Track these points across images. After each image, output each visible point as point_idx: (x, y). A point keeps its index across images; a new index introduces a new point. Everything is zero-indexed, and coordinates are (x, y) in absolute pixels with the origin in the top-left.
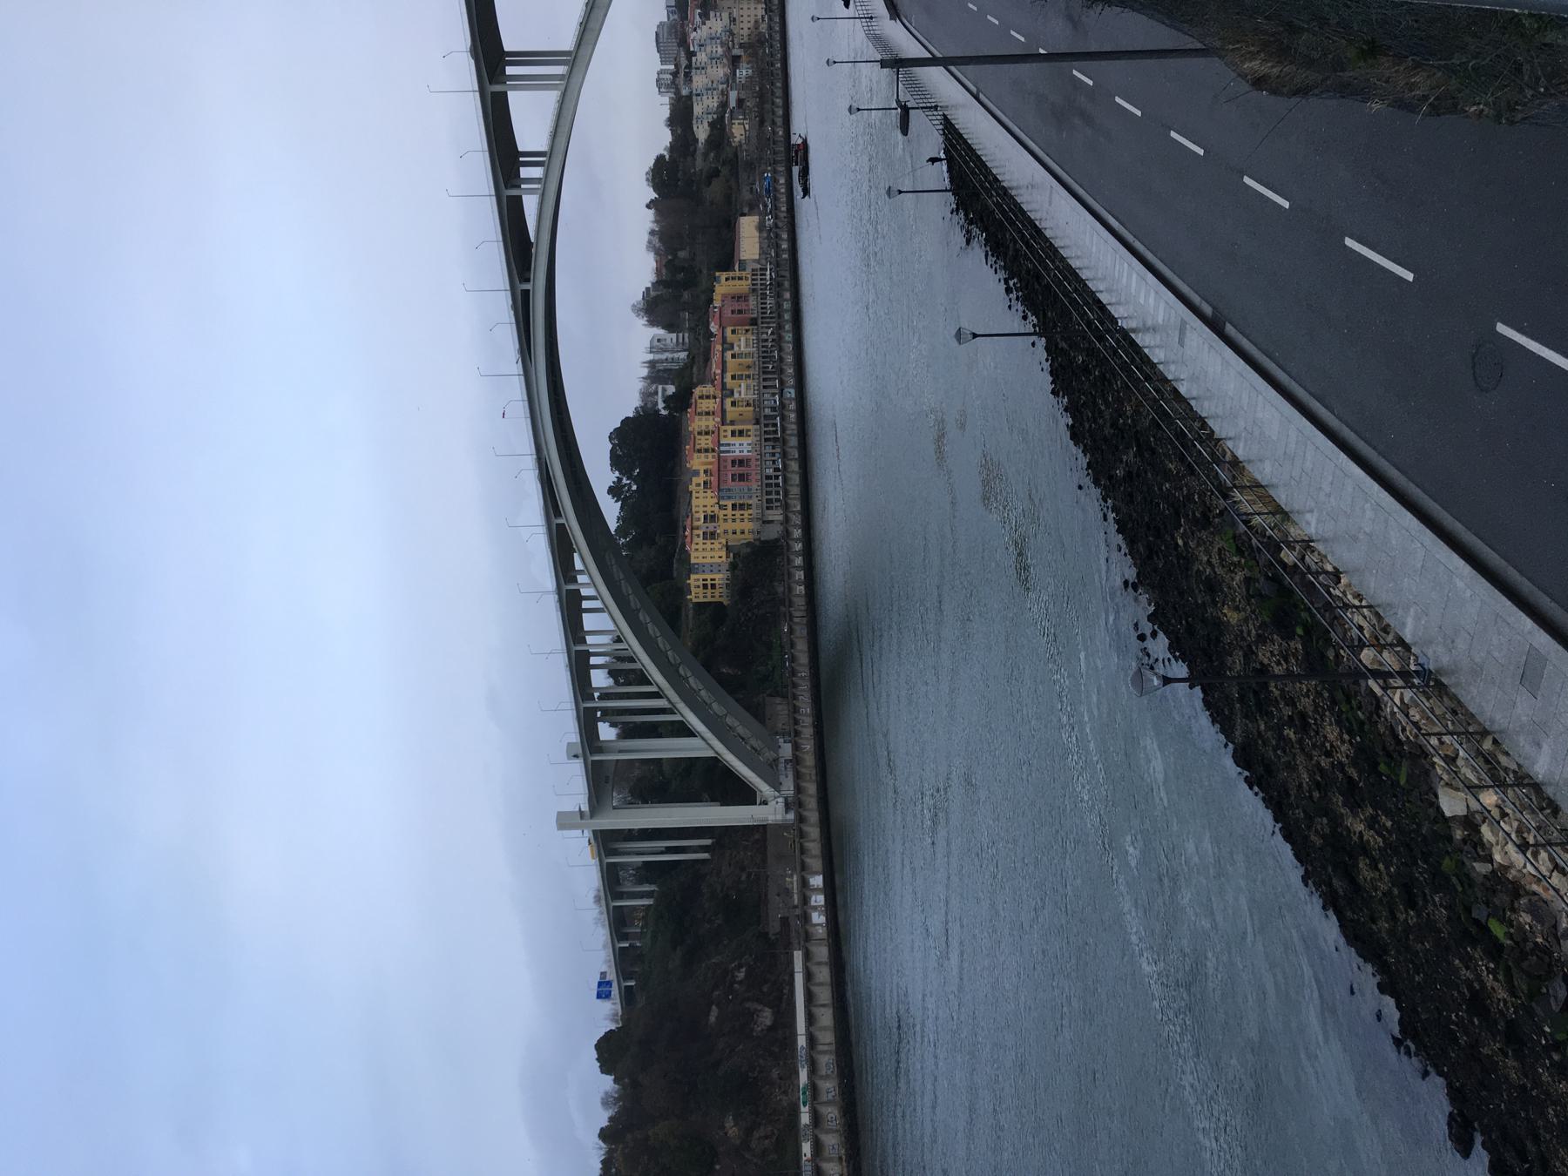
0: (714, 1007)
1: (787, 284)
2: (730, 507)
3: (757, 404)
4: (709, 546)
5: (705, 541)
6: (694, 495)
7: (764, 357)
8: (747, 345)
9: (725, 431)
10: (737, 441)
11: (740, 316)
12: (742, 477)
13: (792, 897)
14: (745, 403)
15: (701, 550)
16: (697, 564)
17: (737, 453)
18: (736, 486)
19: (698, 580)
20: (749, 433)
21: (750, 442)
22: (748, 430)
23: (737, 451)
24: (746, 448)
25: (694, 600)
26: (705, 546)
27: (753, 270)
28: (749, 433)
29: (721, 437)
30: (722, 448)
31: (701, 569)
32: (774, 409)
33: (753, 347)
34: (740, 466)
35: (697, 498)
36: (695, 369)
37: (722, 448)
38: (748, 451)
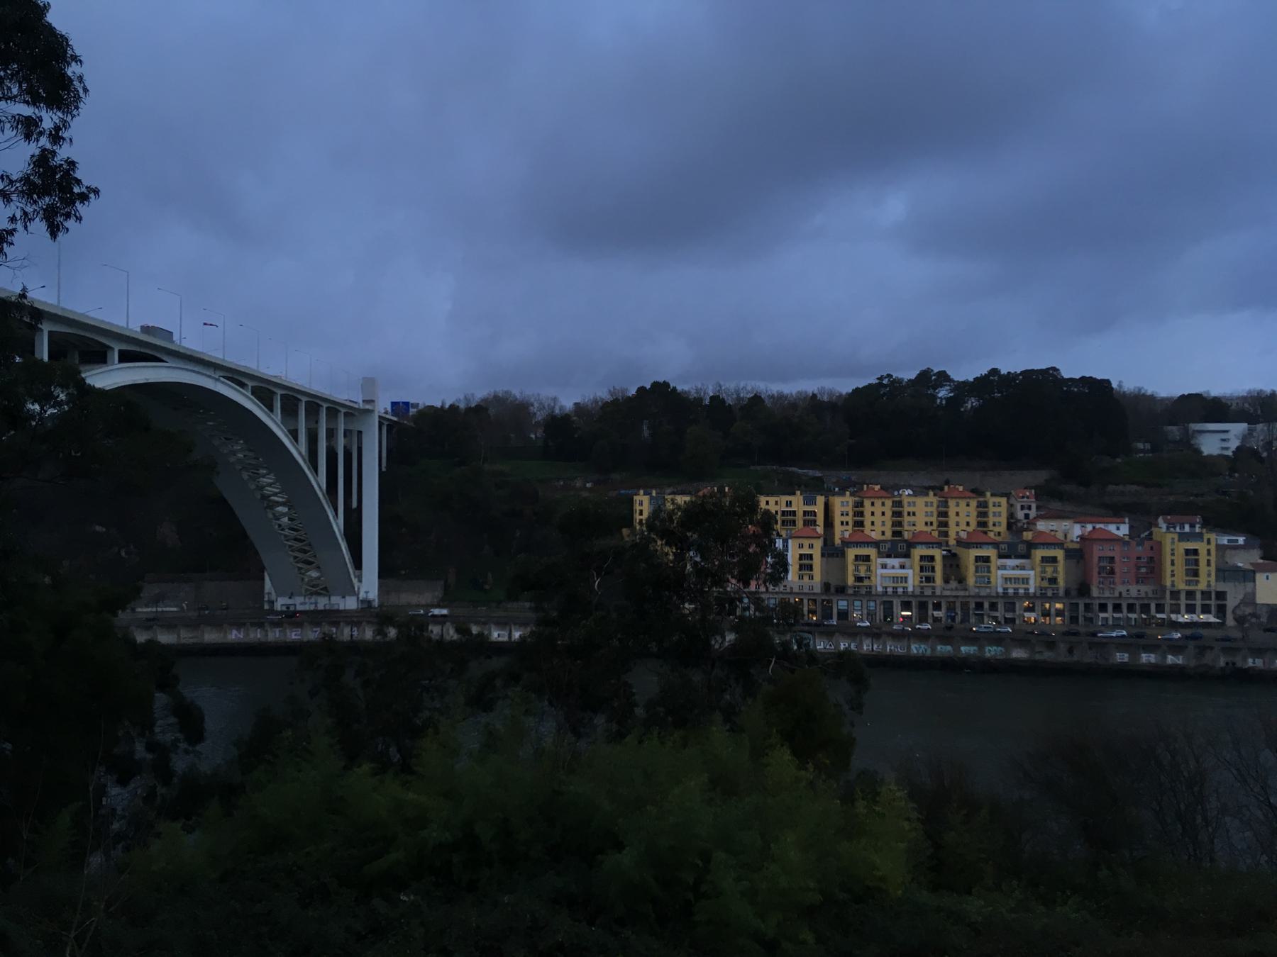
0: (104, 530)
1: (1047, 655)
3: (863, 590)
7: (965, 606)
8: (1007, 579)
9: (811, 546)
11: (1096, 570)
13: (147, 606)
14: (862, 574)
19: (641, 504)
20: (806, 578)
22: (811, 577)
25: (637, 498)
27: (1221, 595)
28: (806, 578)
29: (801, 541)
32: (843, 615)
33: (1006, 589)
36: (1134, 488)
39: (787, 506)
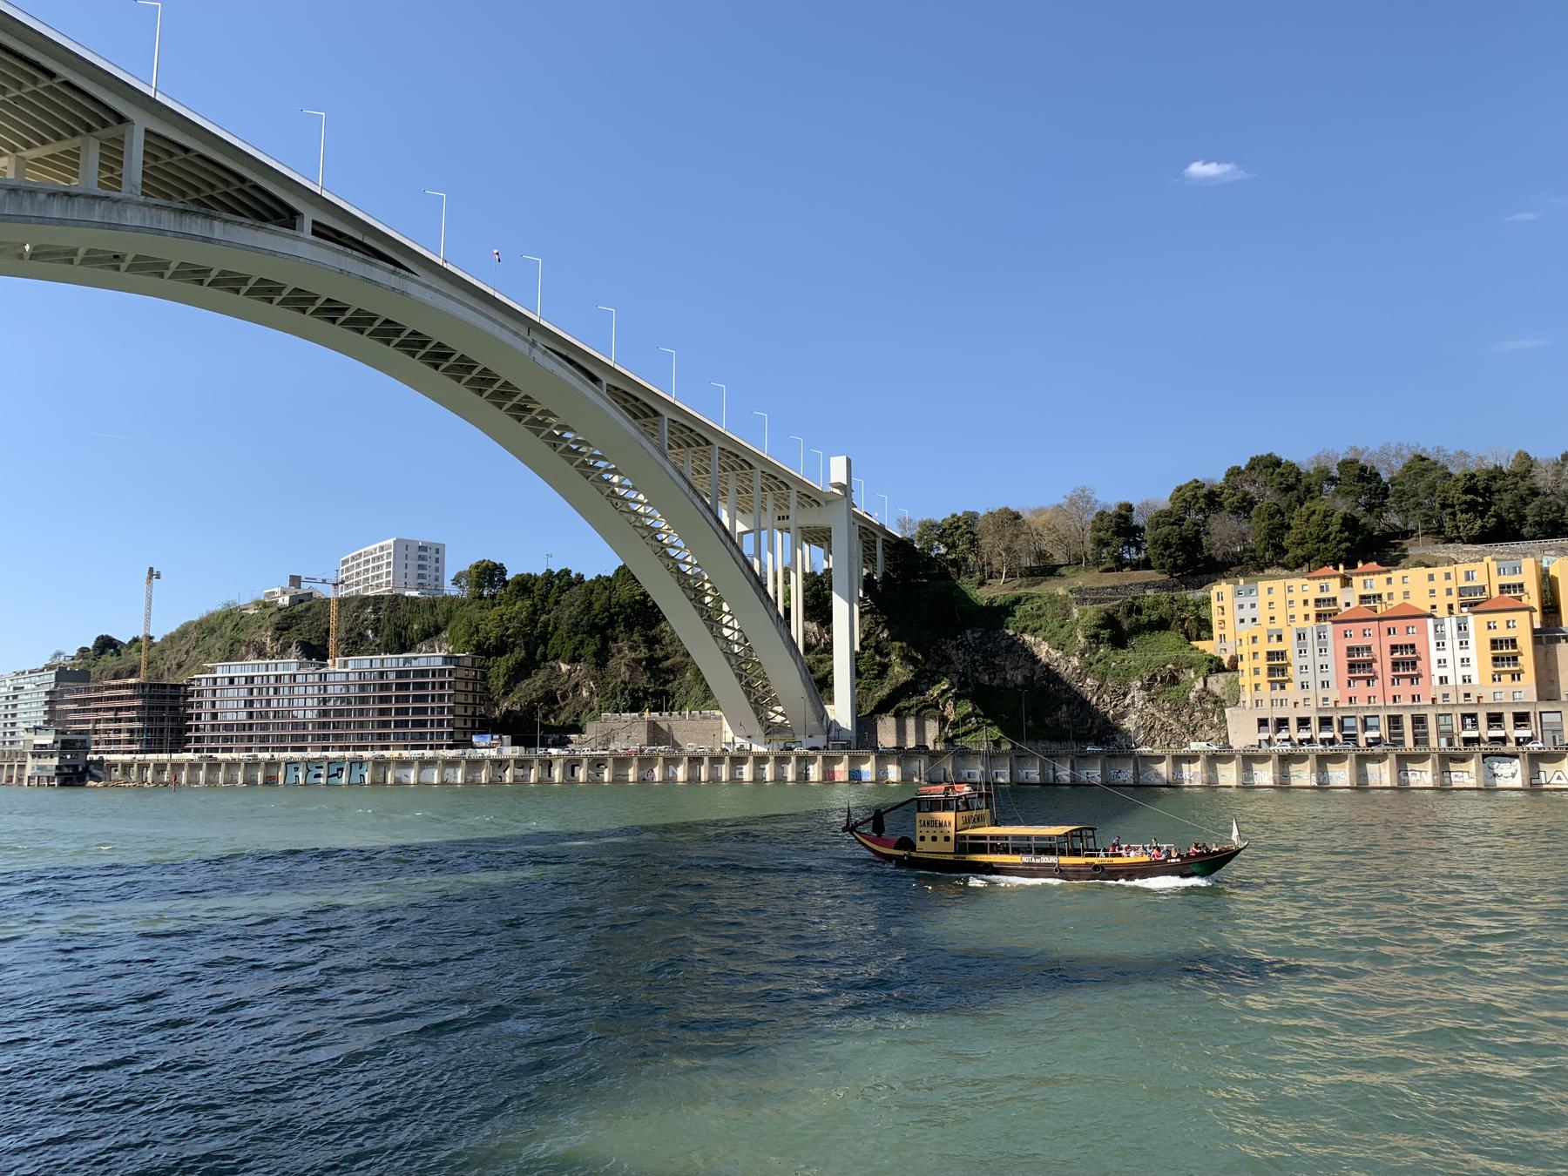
2: (1276, 646)
4: (1299, 610)
5: (1311, 603)
6: (1439, 572)
10: (1479, 653)
12: (1359, 665)
15: (1290, 597)
16: (1257, 594)
17: (1435, 655)
18: (1336, 660)
21: (1475, 681)
23: (1441, 655)
24: (1454, 674)
26: (1299, 603)
30: (1450, 625)
31: (1247, 601)
34: (1396, 665)
35: (1431, 578)
37: (1450, 625)
38: (1443, 680)
39: (1468, 579)
